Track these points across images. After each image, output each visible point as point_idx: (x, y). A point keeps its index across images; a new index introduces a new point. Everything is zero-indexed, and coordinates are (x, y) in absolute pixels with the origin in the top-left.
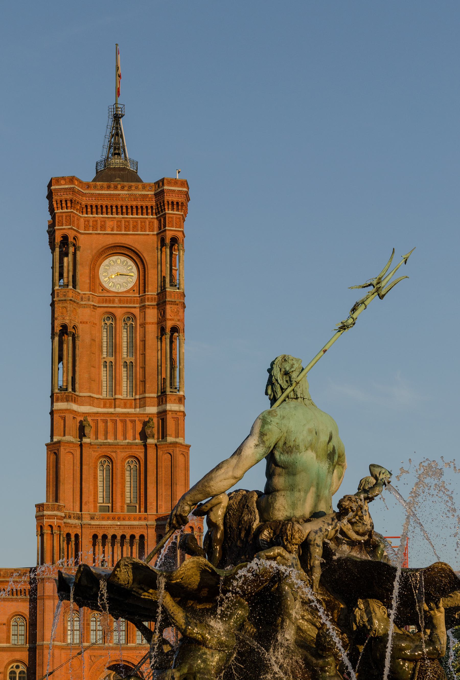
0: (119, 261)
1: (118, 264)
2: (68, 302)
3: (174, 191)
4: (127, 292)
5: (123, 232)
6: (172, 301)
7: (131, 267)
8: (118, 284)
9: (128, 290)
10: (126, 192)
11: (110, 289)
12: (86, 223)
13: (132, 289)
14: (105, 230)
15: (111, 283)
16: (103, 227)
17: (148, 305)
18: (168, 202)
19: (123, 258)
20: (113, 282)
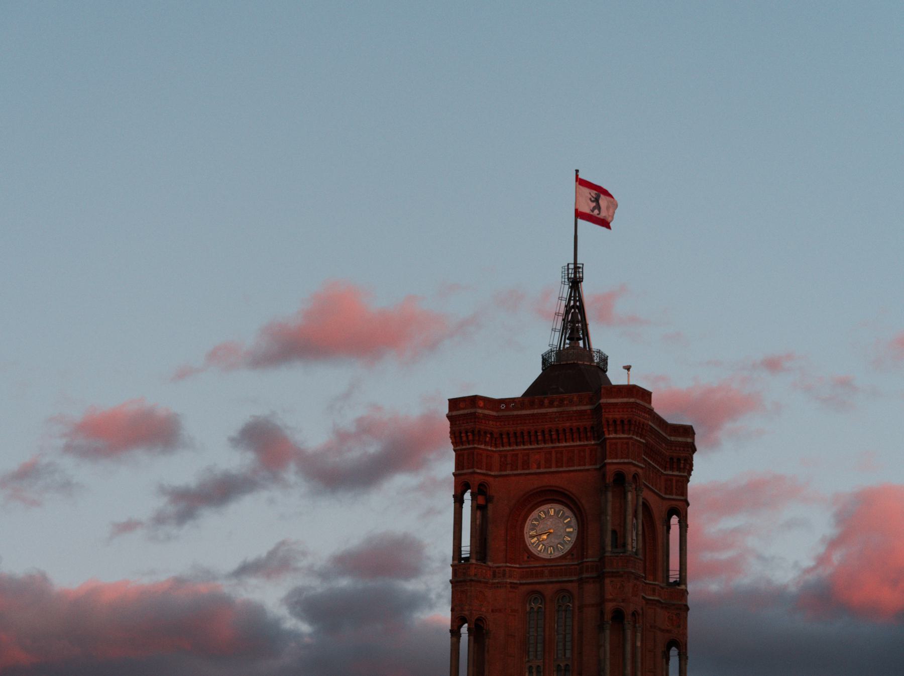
0: (552, 512)
1: (551, 516)
2: (468, 583)
3: (616, 404)
4: (563, 557)
5: (553, 469)
6: (613, 572)
7: (569, 519)
8: (550, 546)
9: (565, 554)
10: (555, 410)
11: (539, 555)
12: (502, 459)
13: (570, 553)
14: (528, 468)
15: (541, 545)
16: (526, 465)
17: (587, 578)
18: (608, 421)
19: (558, 507)
20: (543, 545)
